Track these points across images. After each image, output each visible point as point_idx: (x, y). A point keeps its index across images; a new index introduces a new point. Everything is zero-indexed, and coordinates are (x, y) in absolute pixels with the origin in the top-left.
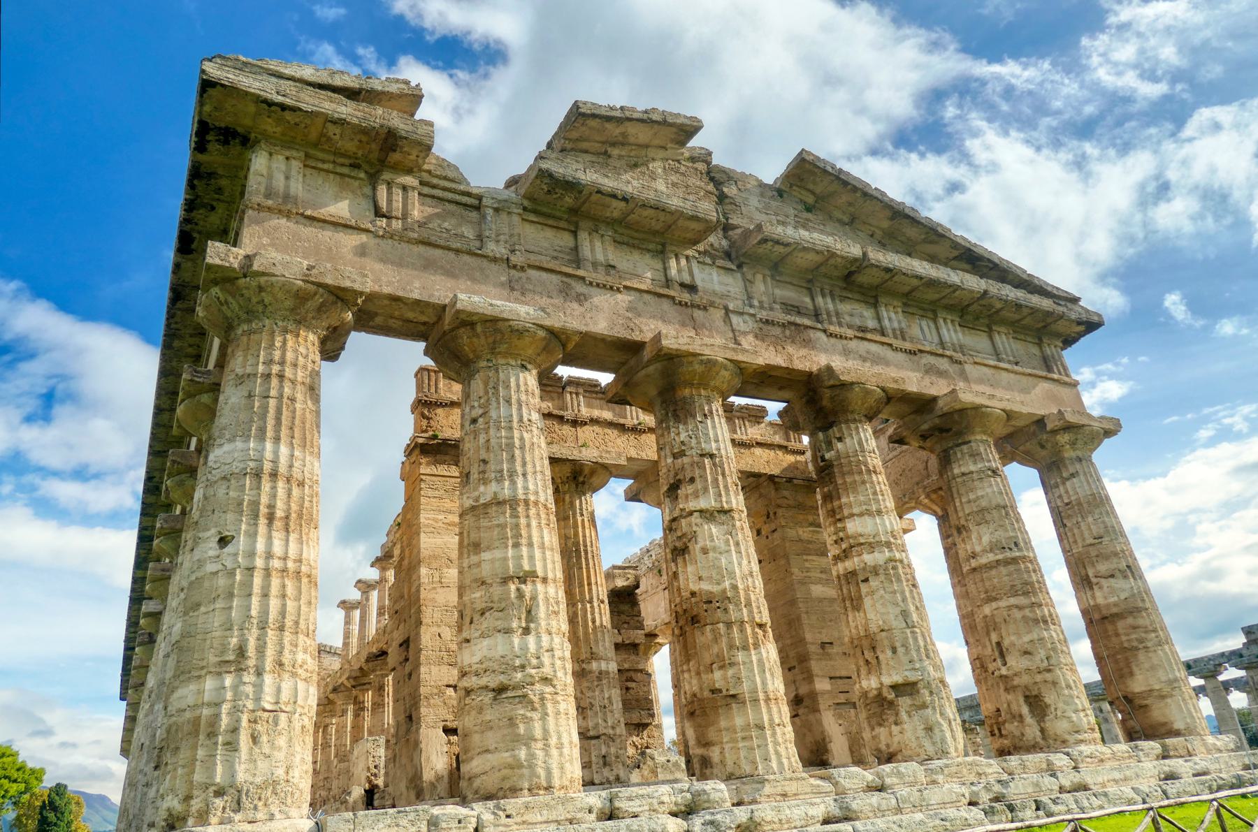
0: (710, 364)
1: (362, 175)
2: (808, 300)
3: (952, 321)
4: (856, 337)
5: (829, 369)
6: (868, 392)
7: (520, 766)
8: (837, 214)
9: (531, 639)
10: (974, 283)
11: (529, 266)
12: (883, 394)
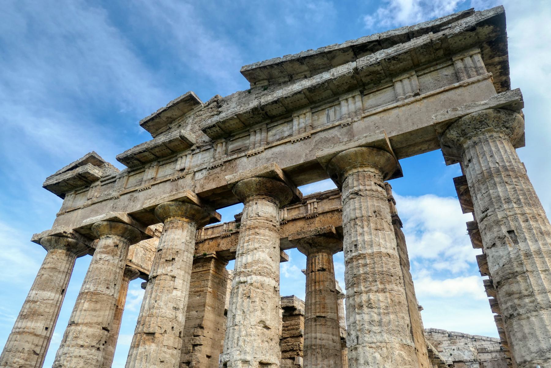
0: (163, 207)
3: (353, 97)
4: (265, 149)
6: (246, 184)
8: (282, 80)
10: (343, 70)
11: (121, 195)
12: (257, 179)
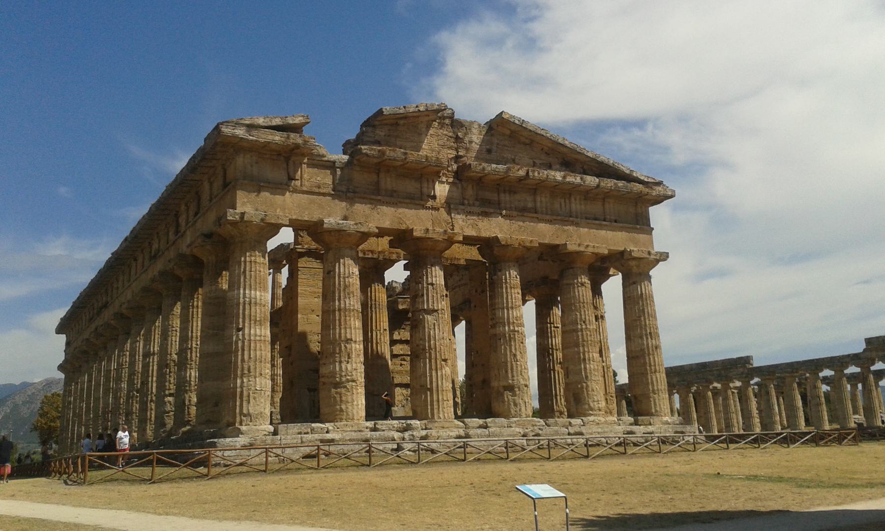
1: (282, 158)
2: (496, 195)
3: (580, 199)
5: (497, 237)
7: (341, 410)
9: (349, 366)
10: (591, 181)
